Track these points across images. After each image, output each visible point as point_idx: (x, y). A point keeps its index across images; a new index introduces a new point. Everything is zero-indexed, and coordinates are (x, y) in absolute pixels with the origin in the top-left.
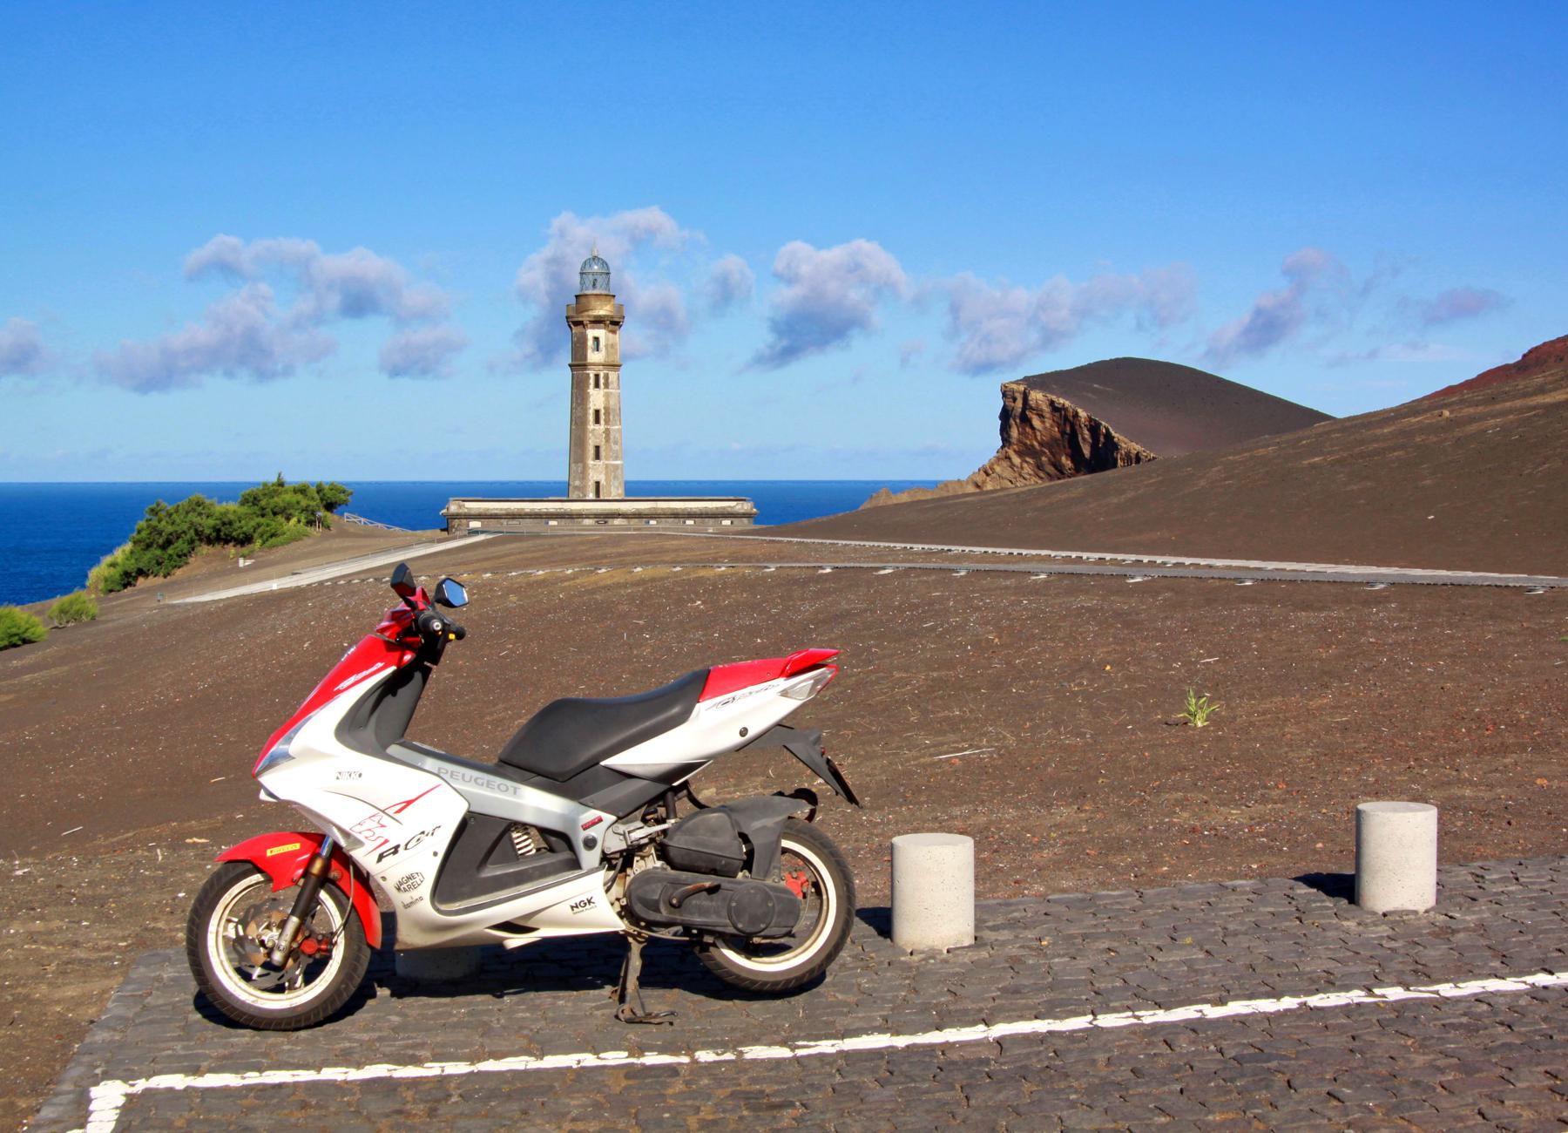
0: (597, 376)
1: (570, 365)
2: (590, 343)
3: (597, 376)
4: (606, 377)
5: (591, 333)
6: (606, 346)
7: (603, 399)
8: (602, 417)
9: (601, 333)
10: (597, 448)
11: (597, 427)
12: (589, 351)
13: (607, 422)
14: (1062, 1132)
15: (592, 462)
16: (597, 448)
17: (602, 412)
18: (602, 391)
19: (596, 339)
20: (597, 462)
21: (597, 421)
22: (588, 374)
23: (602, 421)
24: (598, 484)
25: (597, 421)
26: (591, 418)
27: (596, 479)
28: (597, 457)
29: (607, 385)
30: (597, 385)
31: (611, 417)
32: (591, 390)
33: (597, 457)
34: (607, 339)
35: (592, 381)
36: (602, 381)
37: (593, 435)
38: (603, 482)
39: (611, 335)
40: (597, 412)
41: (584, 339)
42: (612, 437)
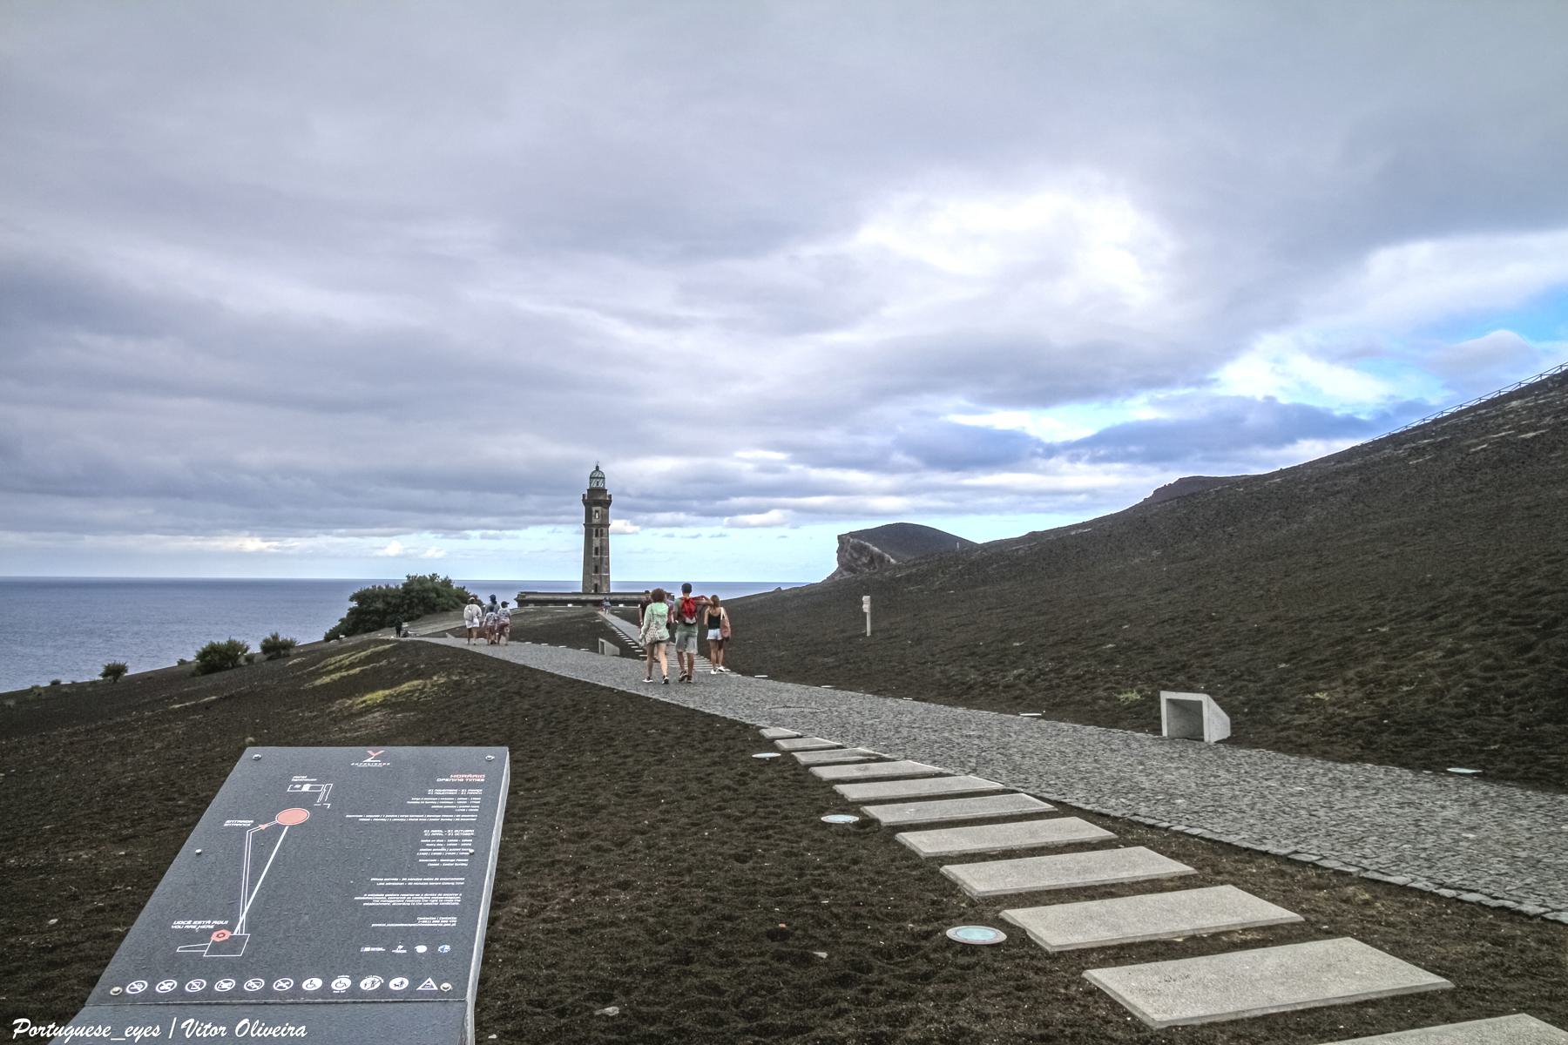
3: (597, 531)
5: (594, 509)
9: (599, 508)
10: (596, 567)
25: (596, 553)
30: (597, 536)
32: (594, 538)
40: (597, 549)
41: (591, 511)
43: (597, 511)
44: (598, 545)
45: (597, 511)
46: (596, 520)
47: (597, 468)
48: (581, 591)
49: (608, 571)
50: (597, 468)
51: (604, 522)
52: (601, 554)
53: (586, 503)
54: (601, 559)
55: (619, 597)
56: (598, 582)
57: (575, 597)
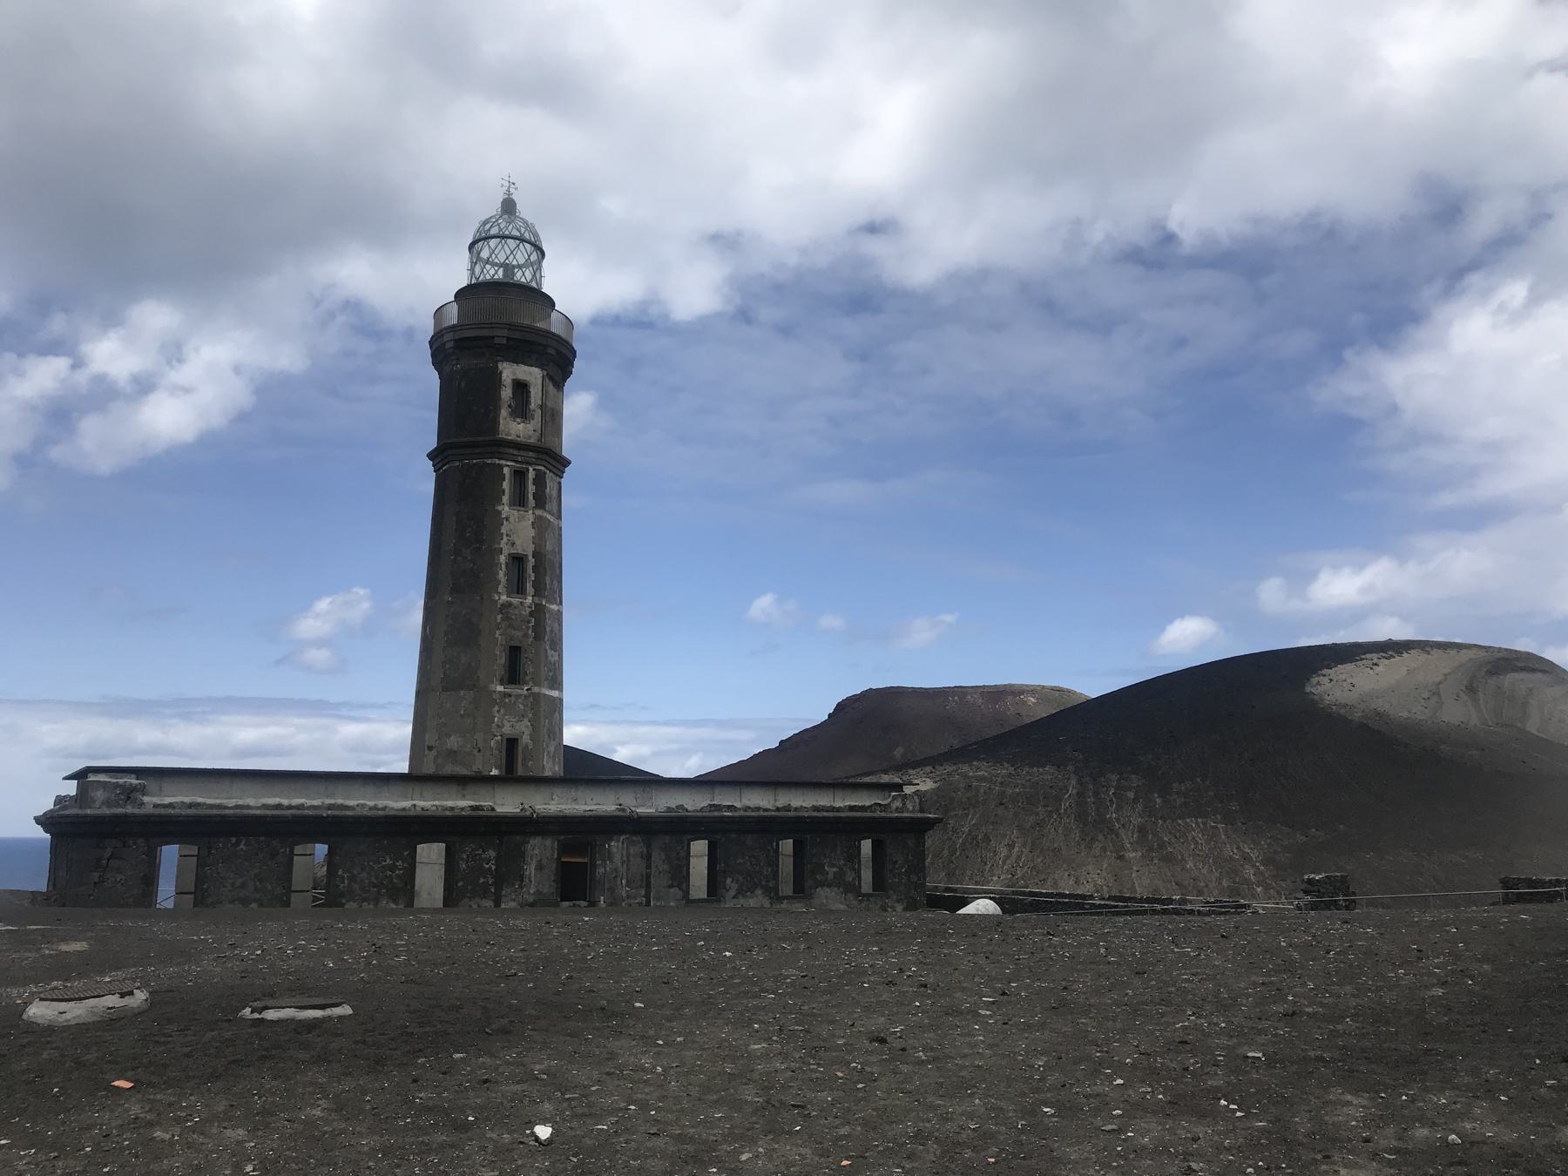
0: (520, 475)
1: (431, 456)
2: (506, 393)
3: (520, 475)
4: (540, 480)
5: (510, 372)
7: (532, 533)
9: (532, 375)
10: (514, 653)
11: (515, 601)
12: (504, 413)
13: (539, 590)
15: (500, 688)
17: (531, 561)
19: (521, 387)
20: (514, 690)
21: (520, 589)
22: (501, 467)
23: (530, 588)
24: (512, 743)
26: (501, 575)
27: (507, 730)
28: (513, 675)
29: (541, 501)
32: (505, 509)
33: (513, 675)
36: (531, 488)
37: (507, 618)
38: (525, 739)
39: (551, 388)
41: (495, 380)
42: (548, 629)
47: (509, 207)
50: (509, 207)
52: (539, 590)
54: (538, 611)
56: (523, 729)
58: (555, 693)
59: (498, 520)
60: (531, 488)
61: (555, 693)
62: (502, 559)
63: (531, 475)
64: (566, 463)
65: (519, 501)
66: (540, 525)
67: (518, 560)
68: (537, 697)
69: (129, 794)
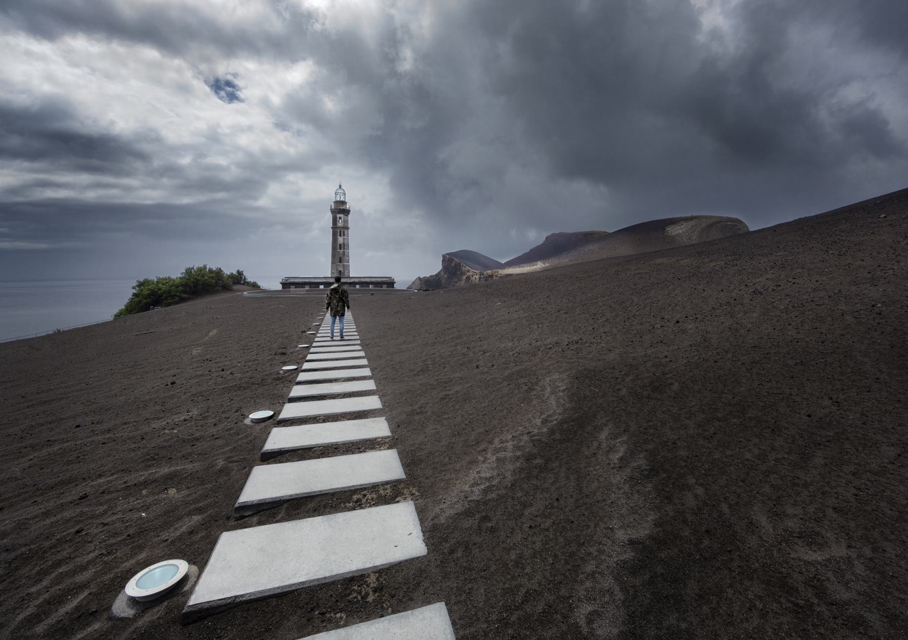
0: (340, 232)
2: (338, 219)
3: (340, 232)
4: (344, 232)
5: (338, 216)
6: (344, 221)
8: (342, 247)
9: (342, 216)
10: (340, 258)
14: (373, 639)
16: (340, 258)
18: (342, 238)
23: (342, 249)
25: (340, 249)
26: (338, 247)
29: (344, 235)
31: (345, 247)
32: (338, 237)
34: (344, 218)
35: (339, 234)
36: (342, 233)
38: (342, 271)
39: (346, 217)
43: (340, 218)
44: (342, 243)
45: (340, 218)
46: (340, 223)
48: (330, 276)
49: (348, 262)
50: (340, 187)
51: (345, 225)
52: (344, 249)
53: (333, 212)
55: (357, 280)
56: (342, 269)
57: (324, 280)
58: (348, 264)
59: (337, 239)
60: (342, 233)
61: (348, 264)
62: (338, 245)
63: (342, 231)
64: (349, 228)
65: (340, 235)
66: (344, 239)
67: (340, 245)
68: (344, 265)
69: (286, 280)
